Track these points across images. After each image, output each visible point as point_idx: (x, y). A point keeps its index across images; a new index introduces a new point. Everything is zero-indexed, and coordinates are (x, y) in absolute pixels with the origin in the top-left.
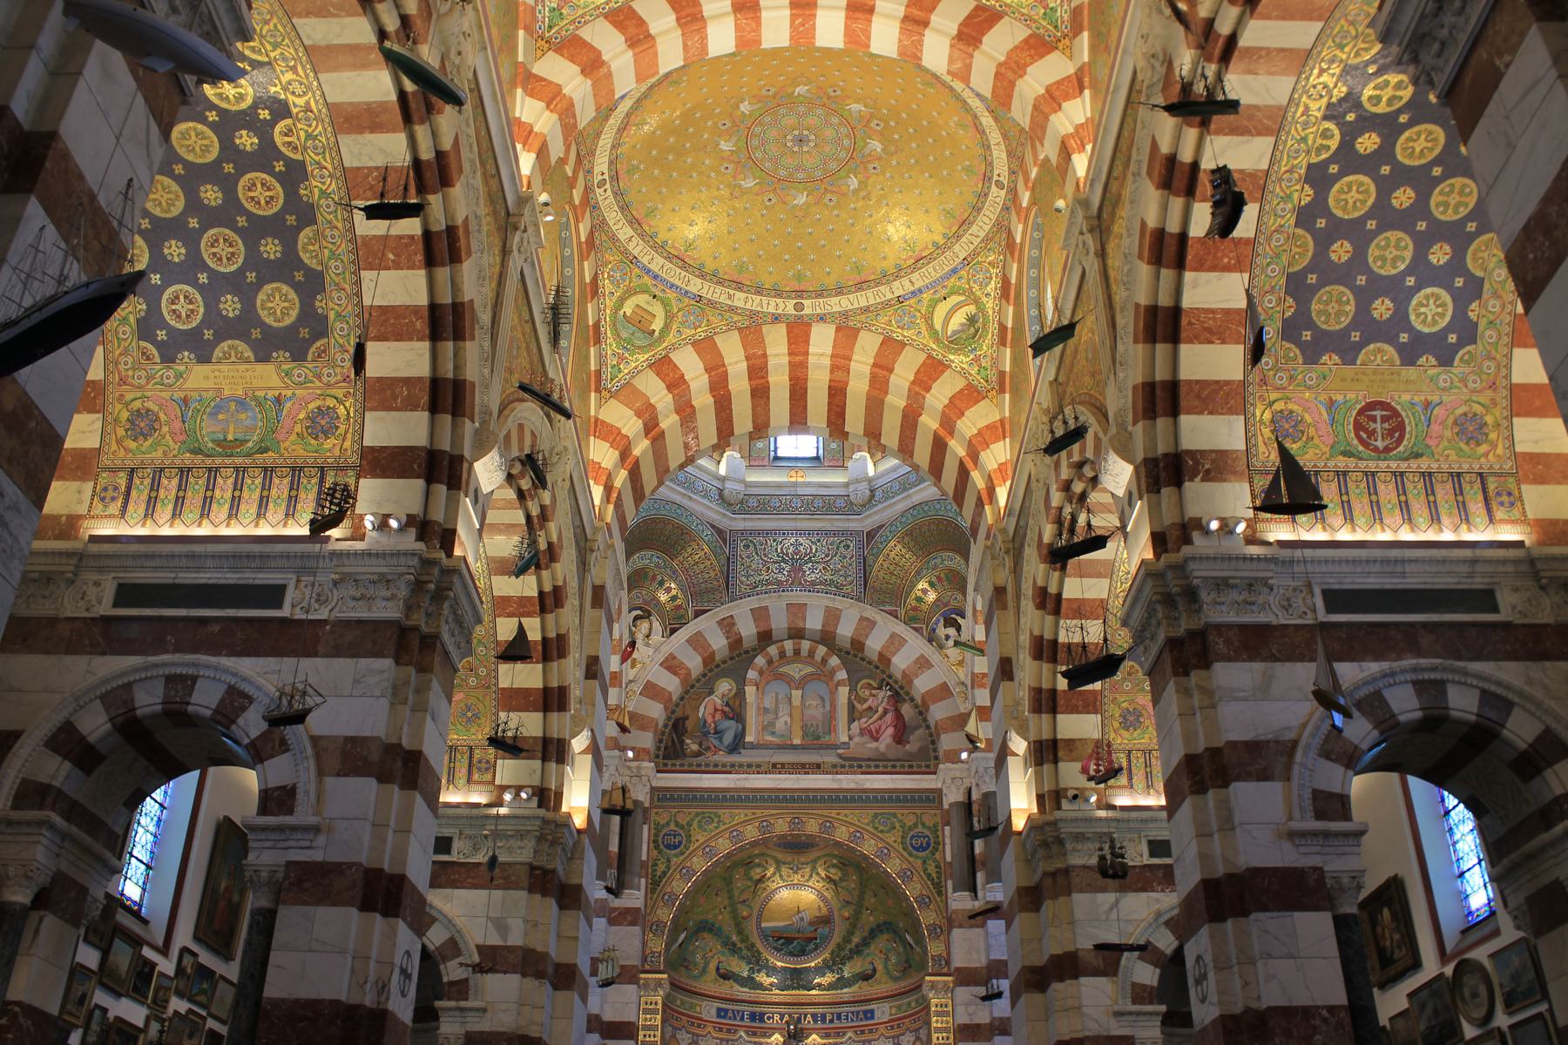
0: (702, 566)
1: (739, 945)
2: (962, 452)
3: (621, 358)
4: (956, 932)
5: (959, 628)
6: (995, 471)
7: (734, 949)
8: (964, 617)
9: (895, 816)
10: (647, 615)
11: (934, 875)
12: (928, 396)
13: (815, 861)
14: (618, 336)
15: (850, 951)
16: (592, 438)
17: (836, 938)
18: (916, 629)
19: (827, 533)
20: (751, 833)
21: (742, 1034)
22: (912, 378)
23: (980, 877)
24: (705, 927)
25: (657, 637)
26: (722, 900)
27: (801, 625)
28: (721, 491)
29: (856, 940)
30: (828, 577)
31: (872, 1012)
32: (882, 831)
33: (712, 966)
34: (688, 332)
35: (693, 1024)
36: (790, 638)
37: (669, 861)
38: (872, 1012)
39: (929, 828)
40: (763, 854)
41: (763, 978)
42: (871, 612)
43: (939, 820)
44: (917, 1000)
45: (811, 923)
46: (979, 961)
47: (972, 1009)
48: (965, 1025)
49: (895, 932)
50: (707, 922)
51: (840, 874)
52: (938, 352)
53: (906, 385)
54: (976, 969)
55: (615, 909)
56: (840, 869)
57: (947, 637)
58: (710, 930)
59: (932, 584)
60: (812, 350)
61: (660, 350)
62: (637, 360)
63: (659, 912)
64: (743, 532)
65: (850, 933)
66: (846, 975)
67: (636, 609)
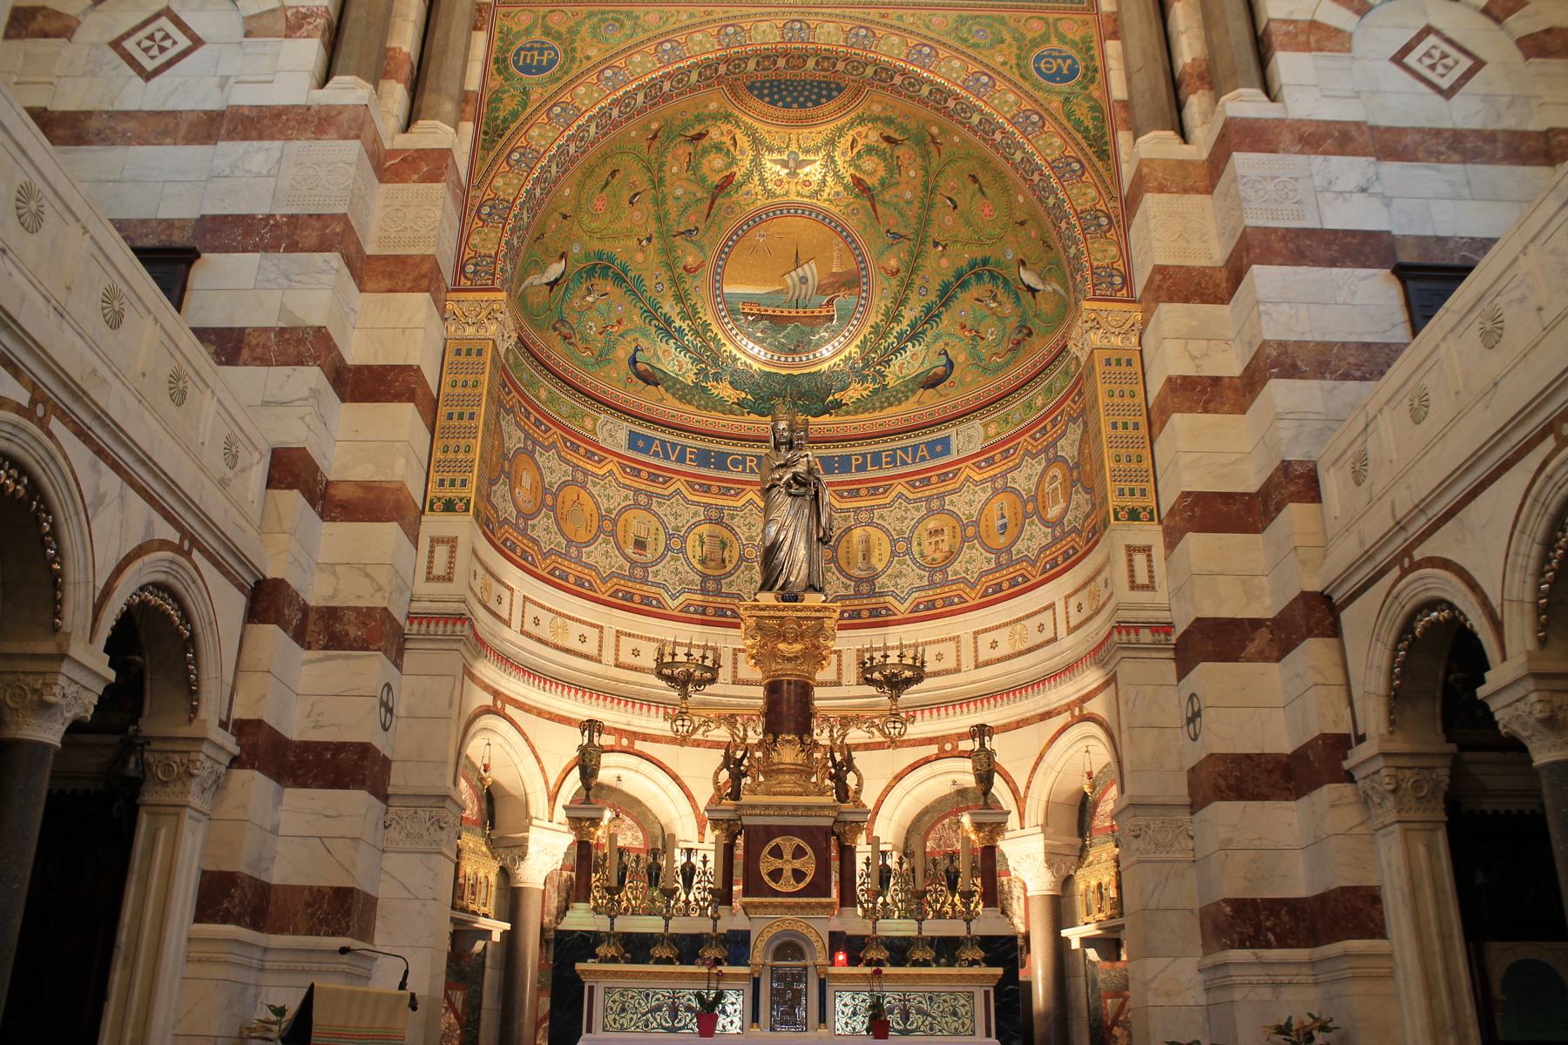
1: (677, 324)
4: (1151, 202)
7: (667, 329)
9: (1002, 21)
11: (1089, 123)
13: (831, 142)
15: (900, 337)
17: (875, 318)
20: (703, 46)
21: (679, 484)
23: (1195, 105)
24: (601, 268)
26: (640, 218)
29: (909, 314)
31: (948, 438)
32: (975, 46)
33: (622, 353)
35: (576, 449)
37: (525, 92)
38: (945, 442)
39: (1073, 44)
40: (727, 117)
41: (725, 391)
43: (1094, 32)
44: (1049, 389)
45: (821, 289)
46: (1212, 253)
47: (1197, 347)
48: (1185, 378)
49: (993, 277)
50: (611, 259)
51: (881, 173)
54: (1202, 271)
55: (393, 153)
56: (882, 155)
58: (620, 279)
63: (499, 182)
65: (901, 301)
66: (891, 382)
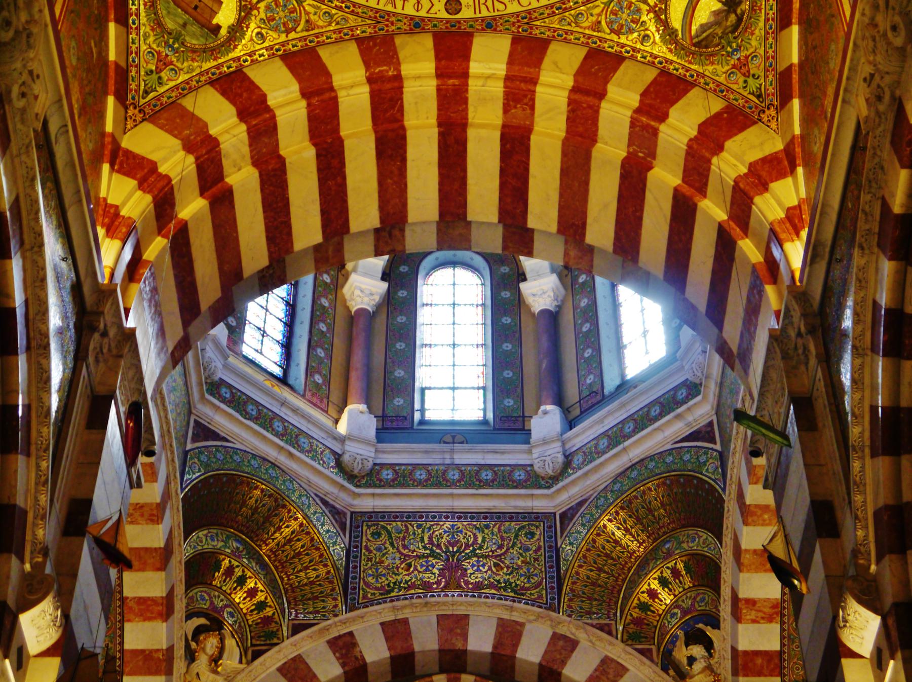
0: (307, 559)
2: (721, 215)
3: (163, 62)
5: (709, 645)
6: (781, 221)
8: (716, 625)
10: (215, 625)
12: (663, 127)
14: (158, 24)
16: (106, 167)
18: (641, 652)
19: (500, 517)
22: (634, 100)
25: (231, 660)
27: (459, 645)
28: (338, 457)
30: (502, 576)
34: (274, 38)
36: (441, 671)
42: (569, 627)
52: (677, 63)
53: (629, 113)
57: (691, 660)
59: (664, 582)
60: (475, 67)
61: (226, 61)
62: (191, 70)
64: (372, 516)
67: (198, 614)
